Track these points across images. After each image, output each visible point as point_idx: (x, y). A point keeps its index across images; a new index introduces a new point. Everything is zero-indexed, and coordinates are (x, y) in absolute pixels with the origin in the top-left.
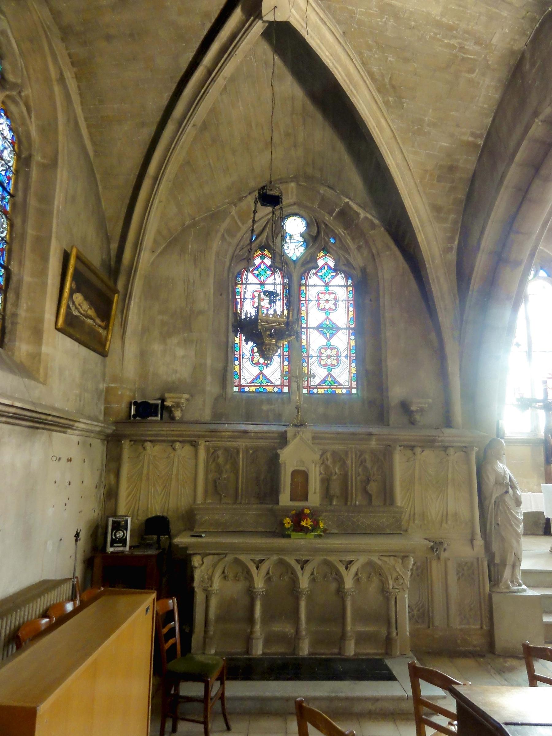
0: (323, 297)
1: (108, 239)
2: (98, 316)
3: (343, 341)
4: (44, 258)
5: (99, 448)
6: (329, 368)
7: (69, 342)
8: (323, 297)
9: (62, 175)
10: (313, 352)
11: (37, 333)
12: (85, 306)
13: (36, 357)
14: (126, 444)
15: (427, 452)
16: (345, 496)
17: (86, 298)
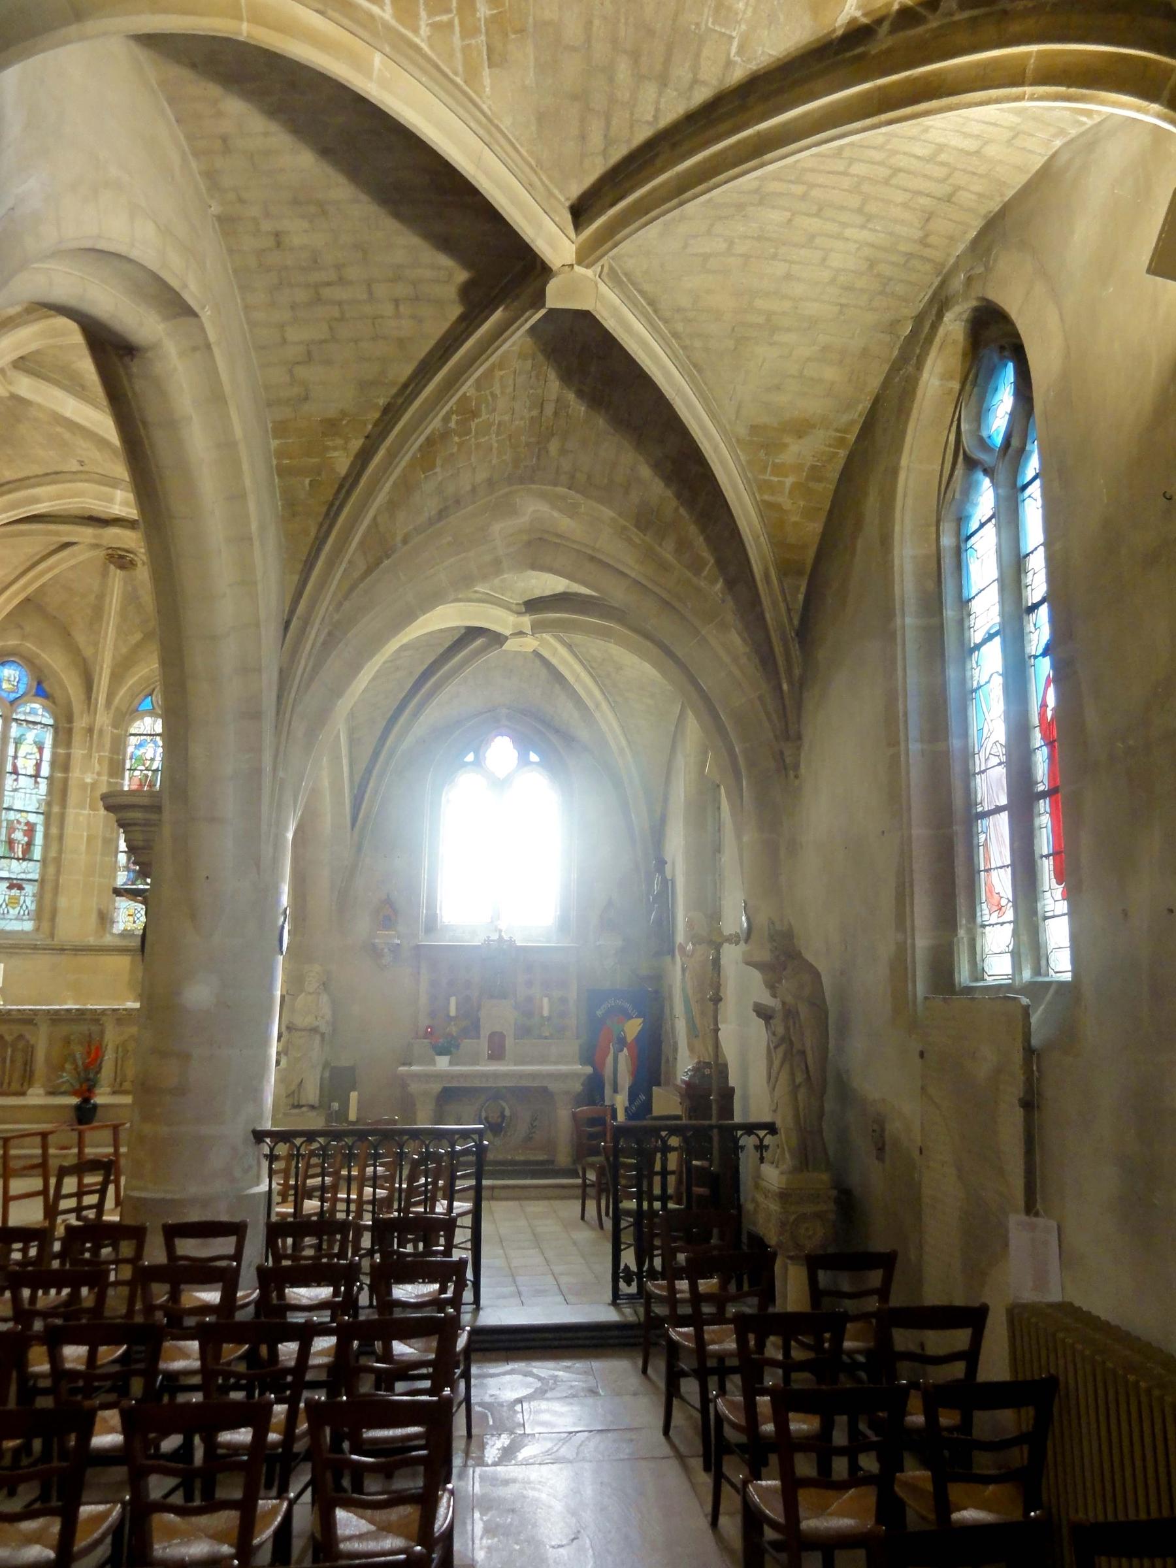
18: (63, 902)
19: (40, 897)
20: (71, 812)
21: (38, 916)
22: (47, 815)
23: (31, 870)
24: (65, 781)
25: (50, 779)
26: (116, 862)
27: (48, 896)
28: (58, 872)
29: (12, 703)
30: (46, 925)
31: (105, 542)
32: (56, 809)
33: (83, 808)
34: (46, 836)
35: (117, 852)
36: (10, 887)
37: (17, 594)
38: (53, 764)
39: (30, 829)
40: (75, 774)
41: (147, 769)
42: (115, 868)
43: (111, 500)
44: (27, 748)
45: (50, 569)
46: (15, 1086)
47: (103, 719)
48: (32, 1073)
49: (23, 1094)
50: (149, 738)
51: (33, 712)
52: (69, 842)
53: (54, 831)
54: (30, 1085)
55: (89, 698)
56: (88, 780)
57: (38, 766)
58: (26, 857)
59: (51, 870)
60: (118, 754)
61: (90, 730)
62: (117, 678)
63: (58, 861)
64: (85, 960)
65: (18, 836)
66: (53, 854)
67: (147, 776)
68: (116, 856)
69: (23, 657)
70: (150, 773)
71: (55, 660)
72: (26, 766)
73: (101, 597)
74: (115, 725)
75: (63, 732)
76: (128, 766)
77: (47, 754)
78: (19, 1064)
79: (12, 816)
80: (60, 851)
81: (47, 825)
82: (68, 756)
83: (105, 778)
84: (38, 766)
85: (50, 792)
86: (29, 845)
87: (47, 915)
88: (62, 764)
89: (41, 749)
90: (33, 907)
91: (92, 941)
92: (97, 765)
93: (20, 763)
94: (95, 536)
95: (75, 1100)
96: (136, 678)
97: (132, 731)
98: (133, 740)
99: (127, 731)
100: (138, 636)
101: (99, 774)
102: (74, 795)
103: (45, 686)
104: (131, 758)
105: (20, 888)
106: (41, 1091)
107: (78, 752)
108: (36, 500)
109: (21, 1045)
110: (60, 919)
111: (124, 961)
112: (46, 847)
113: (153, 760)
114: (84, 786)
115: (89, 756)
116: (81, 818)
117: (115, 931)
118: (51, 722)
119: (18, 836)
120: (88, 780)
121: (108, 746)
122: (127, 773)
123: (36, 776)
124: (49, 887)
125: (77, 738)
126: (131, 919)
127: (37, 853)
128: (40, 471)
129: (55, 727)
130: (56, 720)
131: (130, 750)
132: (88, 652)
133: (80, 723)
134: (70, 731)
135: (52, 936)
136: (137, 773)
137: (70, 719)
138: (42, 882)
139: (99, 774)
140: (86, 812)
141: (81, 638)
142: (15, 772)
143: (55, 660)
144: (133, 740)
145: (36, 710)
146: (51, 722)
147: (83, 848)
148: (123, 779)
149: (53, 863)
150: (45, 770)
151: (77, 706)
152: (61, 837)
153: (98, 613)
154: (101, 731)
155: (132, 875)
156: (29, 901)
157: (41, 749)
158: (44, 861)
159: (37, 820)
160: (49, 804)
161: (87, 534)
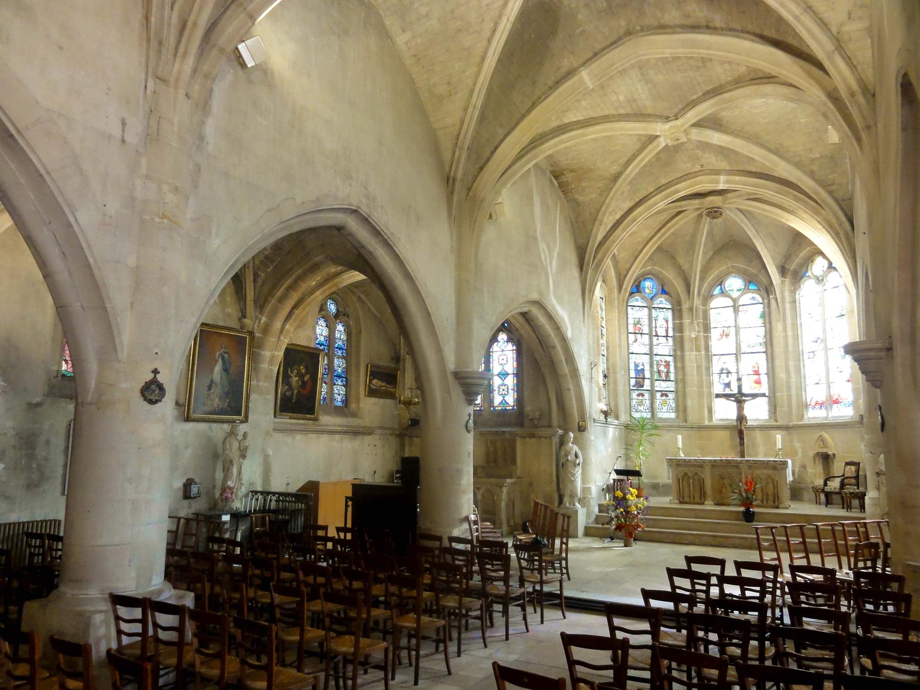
0: (501, 358)
1: (394, 345)
2: (388, 384)
3: (511, 381)
4: (359, 371)
5: (394, 441)
6: (504, 396)
7: (373, 400)
8: (501, 358)
9: (364, 336)
10: (496, 388)
11: (358, 401)
12: (380, 383)
13: (358, 408)
14: (407, 438)
15: (532, 440)
16: (496, 461)
17: (379, 380)
18: (689, 403)
19: (676, 400)
20: (687, 353)
21: (677, 410)
22: (675, 356)
23: (670, 386)
24: (682, 338)
25: (673, 337)
27: (681, 400)
28: (684, 387)
29: (652, 299)
30: (681, 414)
31: (705, 206)
32: (679, 353)
33: (692, 350)
34: (676, 368)
36: (662, 396)
37: (655, 243)
38: (674, 329)
39: (667, 365)
40: (686, 334)
43: (718, 182)
44: (661, 322)
45: (673, 226)
46: (697, 499)
47: (697, 302)
48: (705, 494)
49: (703, 504)
51: (661, 302)
52: (688, 370)
53: (679, 364)
54: (705, 499)
55: (689, 291)
57: (667, 331)
58: (667, 380)
59: (680, 386)
61: (691, 309)
62: (702, 279)
63: (684, 381)
64: (704, 433)
65: (662, 368)
66: (680, 377)
69: (653, 275)
71: (670, 274)
72: (662, 332)
73: (694, 236)
75: (677, 311)
77: (670, 325)
78: (697, 487)
79: (658, 358)
80: (684, 375)
81: (675, 362)
82: (681, 324)
84: (667, 331)
85: (674, 344)
86: (668, 372)
87: (681, 408)
88: (679, 328)
89: (667, 321)
90: (673, 405)
91: (706, 423)
93: (659, 330)
94: (699, 204)
95: (742, 509)
97: (711, 306)
100: (711, 253)
101: (698, 332)
102: (687, 345)
103: (665, 288)
105: (667, 396)
106: (712, 503)
107: (686, 321)
108: (677, 191)
109: (696, 478)
110: (689, 411)
111: (726, 434)
112: (676, 374)
115: (692, 323)
118: (670, 307)
119: (662, 368)
121: (701, 316)
123: (667, 336)
124: (680, 394)
125: (685, 314)
127: (672, 377)
128: (678, 175)
129: (673, 310)
130: (672, 305)
132: (685, 267)
133: (685, 306)
134: (680, 311)
135: (686, 421)
137: (679, 303)
138: (676, 392)
139: (698, 332)
141: (681, 261)
142: (657, 335)
143: (670, 274)
145: (662, 301)
146: (670, 307)
149: (681, 381)
150: (671, 333)
151: (683, 296)
152: (683, 368)
153: (692, 246)
156: (671, 402)
157: (667, 321)
158: (676, 381)
159: (670, 359)
160: (675, 351)
161: (696, 202)
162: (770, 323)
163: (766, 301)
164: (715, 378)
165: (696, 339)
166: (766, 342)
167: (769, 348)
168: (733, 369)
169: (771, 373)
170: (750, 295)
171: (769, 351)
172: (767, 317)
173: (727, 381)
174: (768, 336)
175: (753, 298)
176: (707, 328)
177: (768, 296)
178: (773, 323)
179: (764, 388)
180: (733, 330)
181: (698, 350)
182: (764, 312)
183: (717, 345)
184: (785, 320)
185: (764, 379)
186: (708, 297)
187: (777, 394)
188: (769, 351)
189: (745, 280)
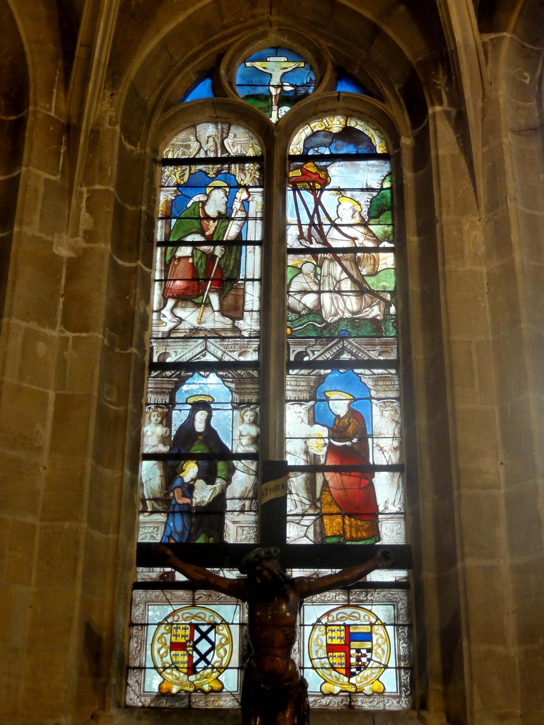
26: (135, 482)
33: (45, 317)
35: (137, 456)
41: (209, 241)
42: (131, 502)
47: (103, 108)
50: (211, 170)
56: (64, 252)
60: (136, 202)
61: (69, 130)
67: (213, 257)
68: (135, 469)
70: (218, 251)
74: (130, 133)
76: (159, 235)
83: (105, 247)
92: (84, 215)
96: (181, 19)
98: (172, 175)
99: (156, 151)
101: (89, 236)
104: (167, 218)
113: (225, 218)
114: (50, 264)
116: (41, 348)
117: (133, 698)
120: (64, 252)
121: (112, 170)
122: (158, 252)
126: (182, 658)
131: (165, 197)
136: (185, 251)
139: (89, 236)
140: (55, 333)
144: (172, 175)
147: (45, 434)
148: (150, 263)
151: (40, 66)
154: (95, 135)
155: (178, 523)
162: (428, 227)
163: (406, 141)
164: (150, 473)
165: (76, 267)
166: (403, 322)
167: (418, 341)
168: (237, 431)
169: (430, 462)
170: (336, 124)
171: (419, 357)
172: (410, 211)
173: (204, 494)
174: (414, 287)
175: (347, 134)
176: (133, 235)
177: (418, 114)
178: (446, 218)
179: (391, 533)
180: (252, 261)
181: (74, 320)
182: (398, 188)
183: (175, 322)
184: (496, 203)
185: (387, 491)
186: (153, 115)
187: (470, 563)
188: (419, 357)
189: (317, 64)
